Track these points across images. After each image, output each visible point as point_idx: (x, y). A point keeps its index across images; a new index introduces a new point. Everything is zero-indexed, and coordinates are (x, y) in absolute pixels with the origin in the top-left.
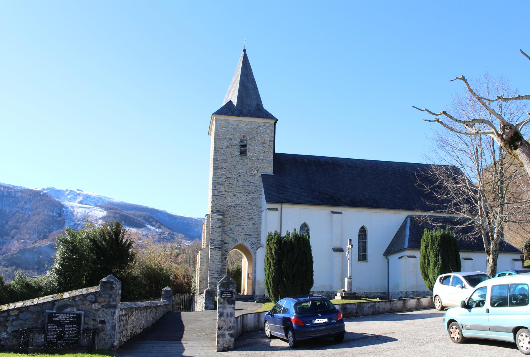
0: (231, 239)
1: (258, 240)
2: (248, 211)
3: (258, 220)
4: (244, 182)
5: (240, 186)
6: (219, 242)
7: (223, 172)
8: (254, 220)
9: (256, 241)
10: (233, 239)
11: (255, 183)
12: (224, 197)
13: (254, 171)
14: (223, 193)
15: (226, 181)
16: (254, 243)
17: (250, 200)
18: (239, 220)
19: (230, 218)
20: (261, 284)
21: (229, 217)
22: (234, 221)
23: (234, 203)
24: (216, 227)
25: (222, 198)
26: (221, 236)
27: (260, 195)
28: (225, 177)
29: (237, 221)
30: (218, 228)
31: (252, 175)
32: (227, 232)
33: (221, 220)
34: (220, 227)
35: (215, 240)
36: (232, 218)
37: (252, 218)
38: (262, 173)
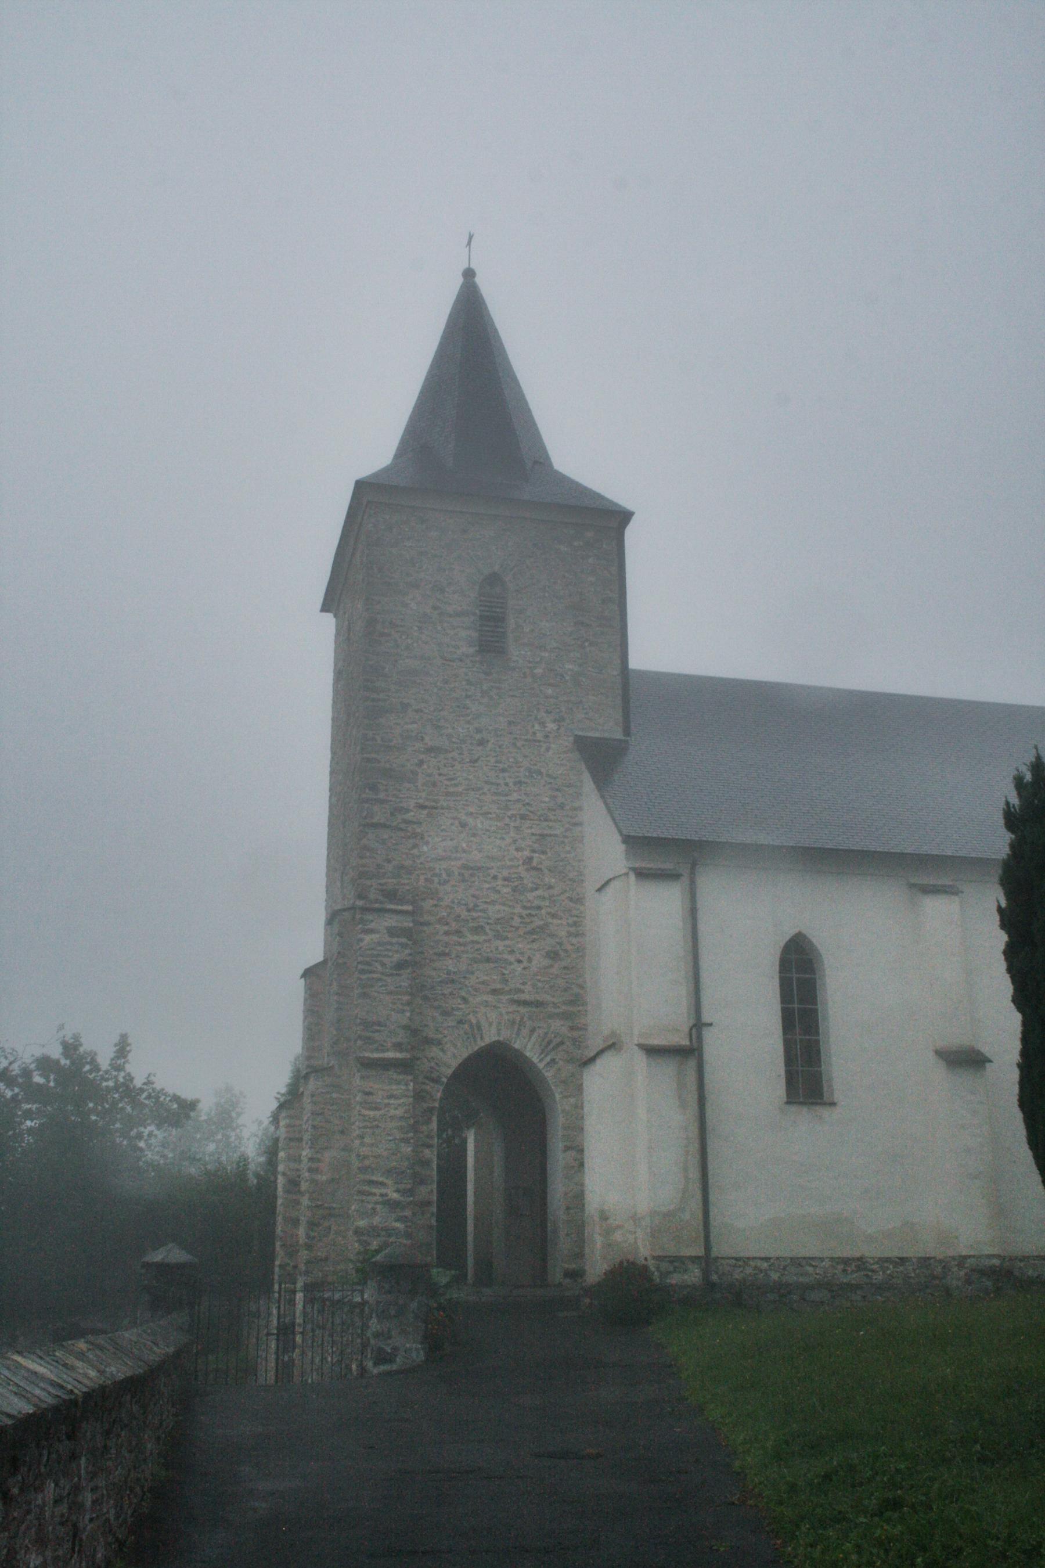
0: (451, 1022)
1: (572, 1028)
2: (522, 898)
3: (570, 934)
4: (503, 770)
5: (486, 788)
6: (401, 1036)
7: (410, 726)
8: (552, 935)
9: (564, 1030)
10: (460, 1022)
11: (548, 776)
12: (415, 835)
13: (543, 724)
14: (409, 816)
15: (421, 763)
16: (558, 1040)
17: (529, 846)
18: (487, 934)
19: (446, 928)
20: (619, 1227)
21: (442, 921)
22: (461, 940)
23: (460, 859)
24: (383, 965)
25: (409, 838)
26: (406, 1008)
27: (576, 824)
28: (419, 745)
29: (476, 938)
30: (391, 968)
31: (534, 741)
32: (432, 988)
33: (407, 933)
34: (400, 966)
35: (379, 1024)
36: (454, 925)
37: (542, 928)
38: (576, 733)
